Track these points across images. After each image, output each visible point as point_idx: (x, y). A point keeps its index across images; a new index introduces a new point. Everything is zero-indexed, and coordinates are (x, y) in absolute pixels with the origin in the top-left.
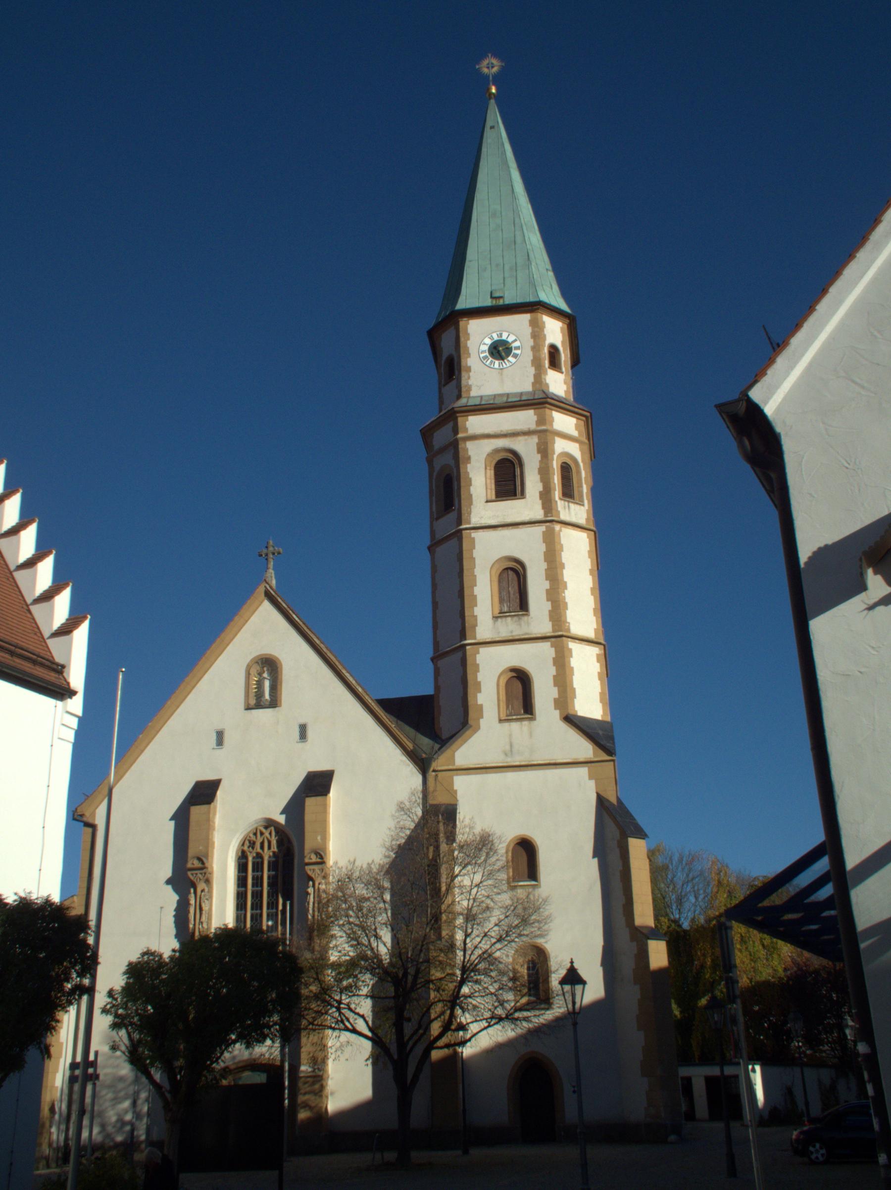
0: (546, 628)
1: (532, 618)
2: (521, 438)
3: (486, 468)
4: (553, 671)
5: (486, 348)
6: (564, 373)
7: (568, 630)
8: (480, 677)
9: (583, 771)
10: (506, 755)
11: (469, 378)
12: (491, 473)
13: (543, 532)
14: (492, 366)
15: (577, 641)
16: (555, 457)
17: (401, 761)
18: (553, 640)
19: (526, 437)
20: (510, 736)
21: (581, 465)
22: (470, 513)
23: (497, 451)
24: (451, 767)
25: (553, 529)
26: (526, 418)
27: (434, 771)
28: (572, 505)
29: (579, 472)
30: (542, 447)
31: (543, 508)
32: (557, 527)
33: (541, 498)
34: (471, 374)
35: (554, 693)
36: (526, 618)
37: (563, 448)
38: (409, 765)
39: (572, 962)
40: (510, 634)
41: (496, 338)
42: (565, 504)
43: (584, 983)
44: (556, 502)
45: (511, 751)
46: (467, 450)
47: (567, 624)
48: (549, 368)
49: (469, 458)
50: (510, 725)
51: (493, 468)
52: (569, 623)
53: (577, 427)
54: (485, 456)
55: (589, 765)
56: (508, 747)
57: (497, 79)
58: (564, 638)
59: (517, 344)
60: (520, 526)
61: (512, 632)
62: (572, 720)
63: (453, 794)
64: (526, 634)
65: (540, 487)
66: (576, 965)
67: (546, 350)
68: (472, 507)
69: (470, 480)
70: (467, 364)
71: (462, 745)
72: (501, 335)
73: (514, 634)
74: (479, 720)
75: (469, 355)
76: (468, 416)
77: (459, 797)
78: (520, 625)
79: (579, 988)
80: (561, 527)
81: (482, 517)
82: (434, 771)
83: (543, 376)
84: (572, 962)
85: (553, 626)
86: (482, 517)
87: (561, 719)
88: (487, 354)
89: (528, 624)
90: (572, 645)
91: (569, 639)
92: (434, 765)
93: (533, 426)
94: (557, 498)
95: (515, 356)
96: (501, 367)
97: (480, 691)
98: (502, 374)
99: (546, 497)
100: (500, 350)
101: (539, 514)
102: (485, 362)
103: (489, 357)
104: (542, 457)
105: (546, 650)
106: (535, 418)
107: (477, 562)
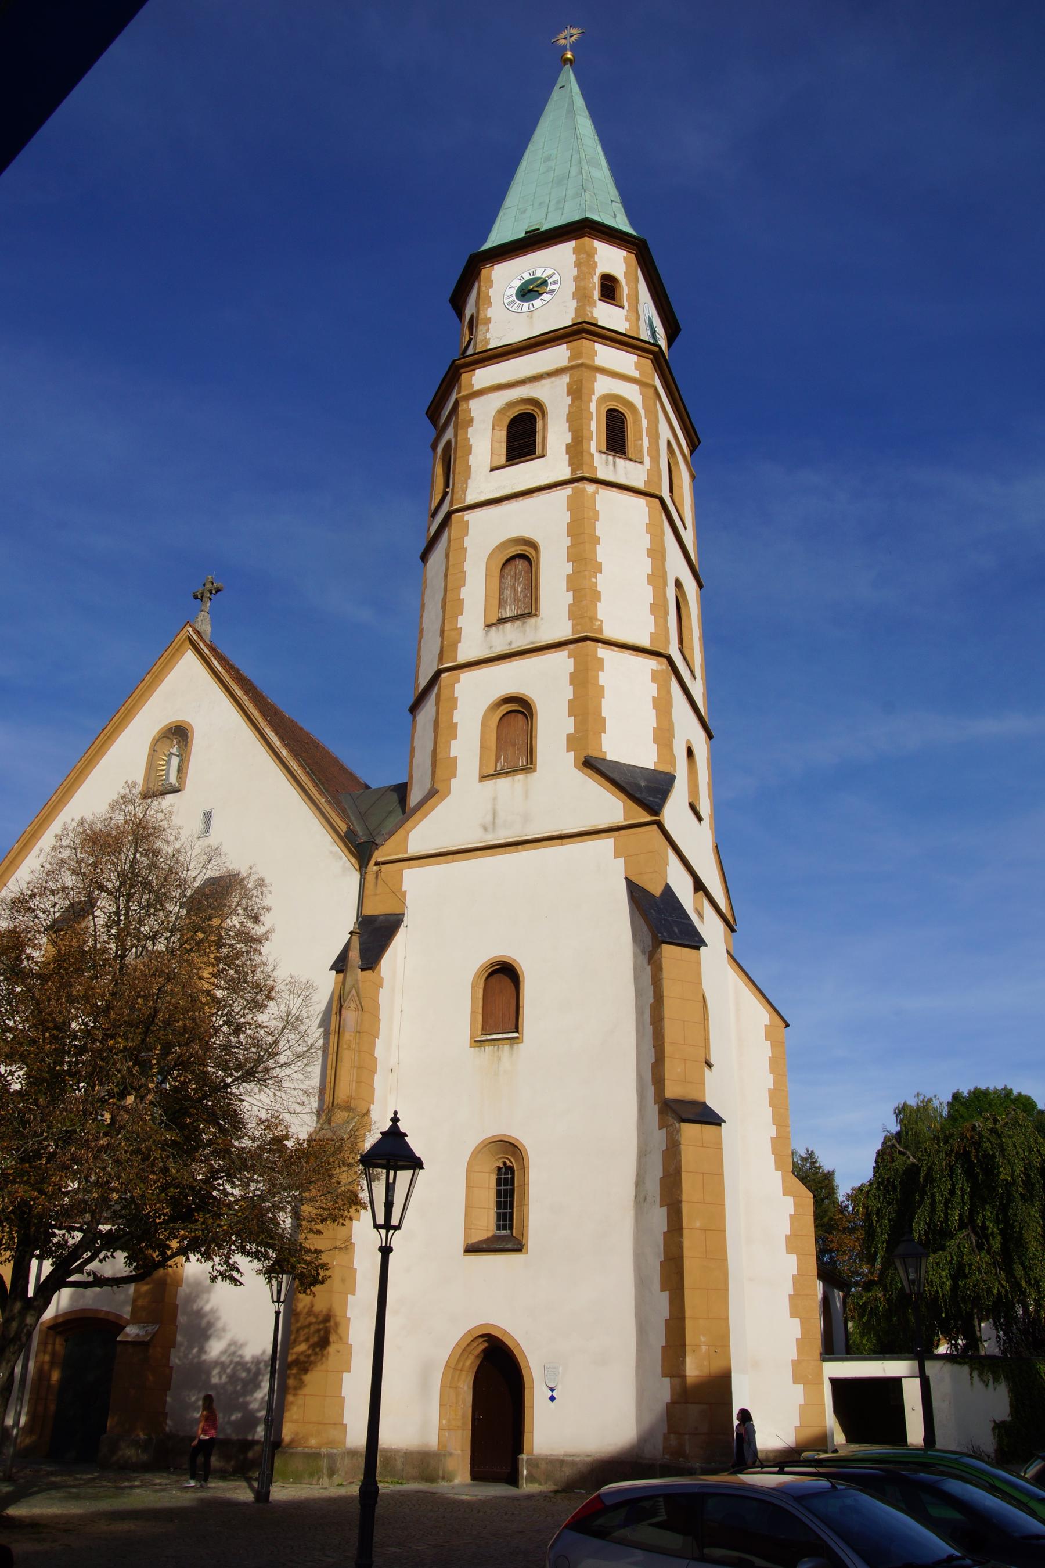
0: (564, 631)
1: (542, 619)
2: (546, 382)
3: (493, 429)
4: (569, 693)
5: (514, 291)
6: (626, 307)
7: (600, 630)
8: (457, 717)
9: (607, 844)
10: (485, 829)
11: (488, 330)
12: (503, 435)
13: (568, 496)
14: (519, 311)
15: (615, 648)
16: (594, 398)
17: (331, 852)
18: (572, 646)
19: (553, 379)
20: (495, 799)
21: (642, 412)
22: (464, 491)
23: (510, 405)
24: (400, 856)
25: (584, 490)
26: (558, 355)
27: (377, 864)
28: (620, 462)
29: (637, 422)
30: (575, 387)
31: (571, 464)
32: (591, 488)
33: (567, 453)
34: (490, 326)
35: (569, 725)
36: (532, 620)
37: (611, 389)
38: (341, 858)
39: (395, 1120)
40: (508, 648)
41: (527, 277)
42: (607, 460)
43: (416, 1164)
44: (592, 455)
45: (494, 823)
46: (470, 410)
47: (598, 623)
48: (600, 300)
49: (471, 420)
50: (495, 783)
51: (505, 429)
52: (602, 621)
53: (637, 366)
54: (493, 413)
55: (617, 833)
56: (489, 818)
57: (573, 47)
58: (589, 643)
59: (556, 277)
60: (535, 494)
61: (510, 644)
62: (593, 765)
63: (400, 896)
64: (532, 643)
65: (568, 438)
66: (403, 1127)
67: (596, 280)
68: (469, 481)
69: (470, 447)
70: (486, 315)
71: (420, 820)
72: (534, 273)
73: (513, 646)
74: (450, 780)
75: (490, 304)
76: (475, 370)
77: (409, 901)
78: (524, 632)
79: (403, 1176)
80: (597, 488)
81: (482, 492)
82: (377, 864)
83: (588, 308)
84: (395, 1120)
85: (573, 626)
86: (482, 492)
87: (575, 766)
88: (514, 298)
89: (536, 628)
90: (602, 652)
91: (600, 645)
92: (379, 855)
93: (564, 363)
94: (593, 449)
95: (552, 292)
96: (532, 309)
97: (455, 738)
98: (531, 317)
99: (576, 451)
100: (529, 291)
101: (566, 474)
102: (509, 308)
103: (516, 301)
104: (573, 400)
105: (562, 662)
106: (568, 353)
107: (469, 553)
